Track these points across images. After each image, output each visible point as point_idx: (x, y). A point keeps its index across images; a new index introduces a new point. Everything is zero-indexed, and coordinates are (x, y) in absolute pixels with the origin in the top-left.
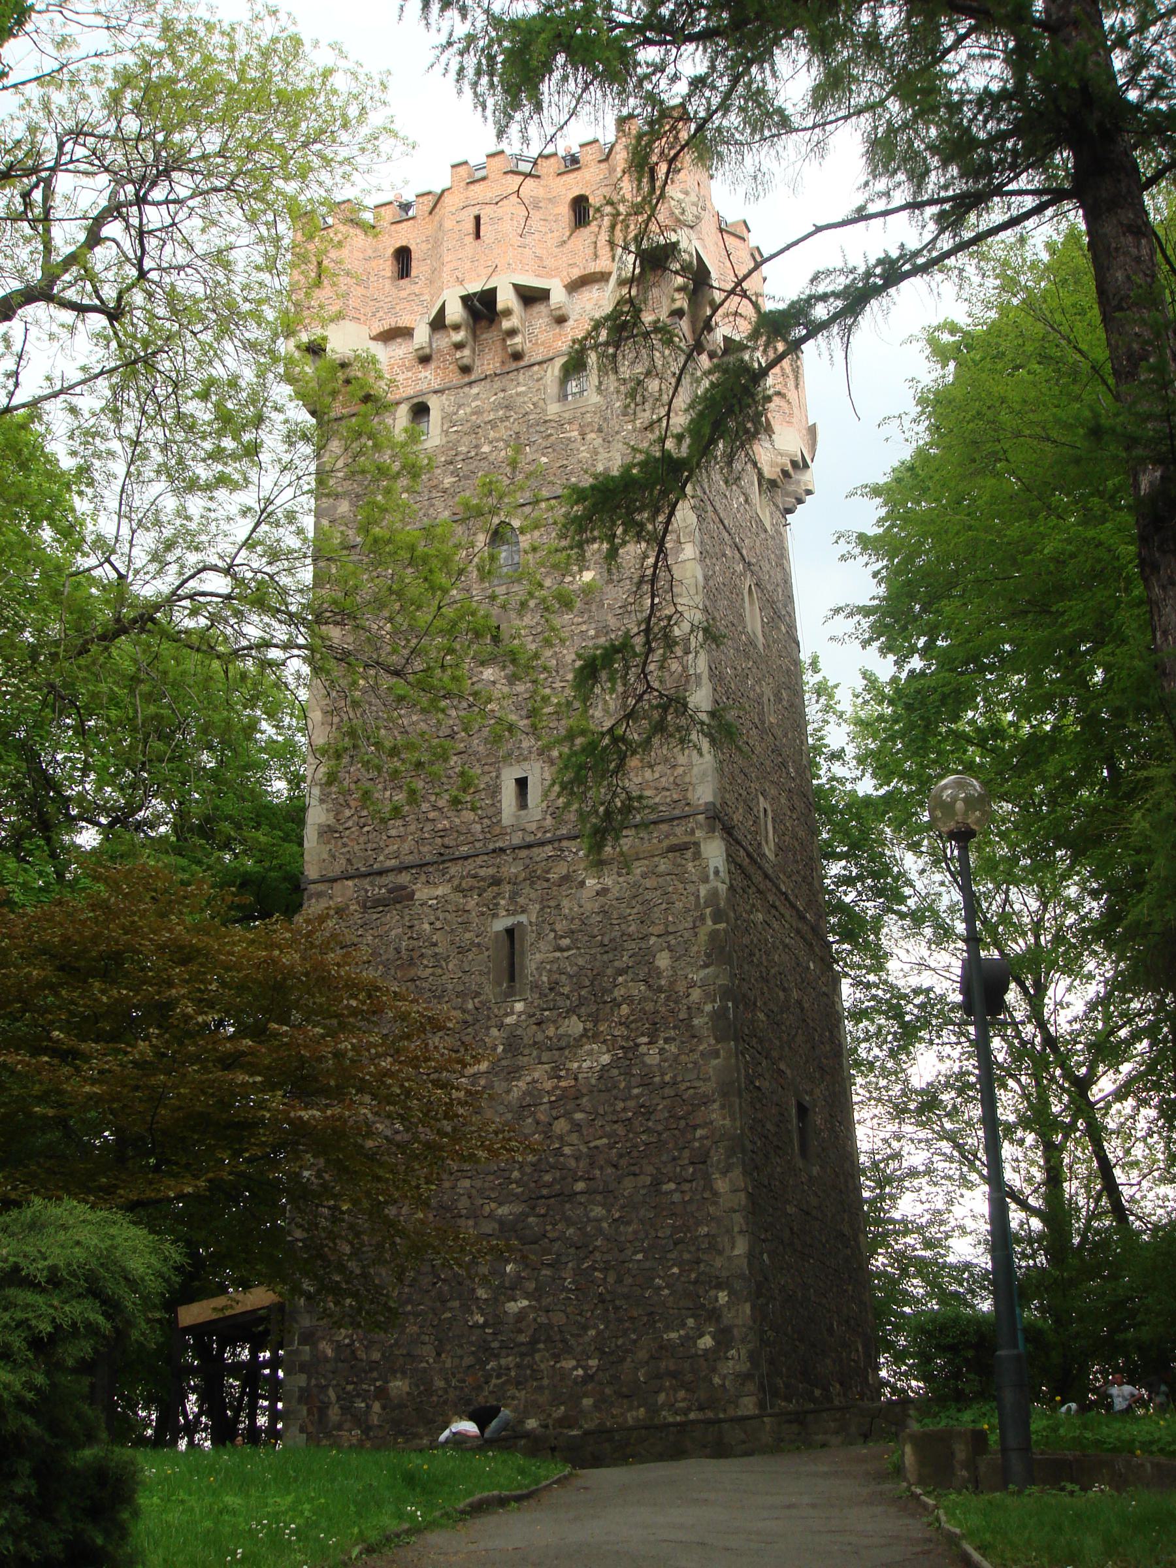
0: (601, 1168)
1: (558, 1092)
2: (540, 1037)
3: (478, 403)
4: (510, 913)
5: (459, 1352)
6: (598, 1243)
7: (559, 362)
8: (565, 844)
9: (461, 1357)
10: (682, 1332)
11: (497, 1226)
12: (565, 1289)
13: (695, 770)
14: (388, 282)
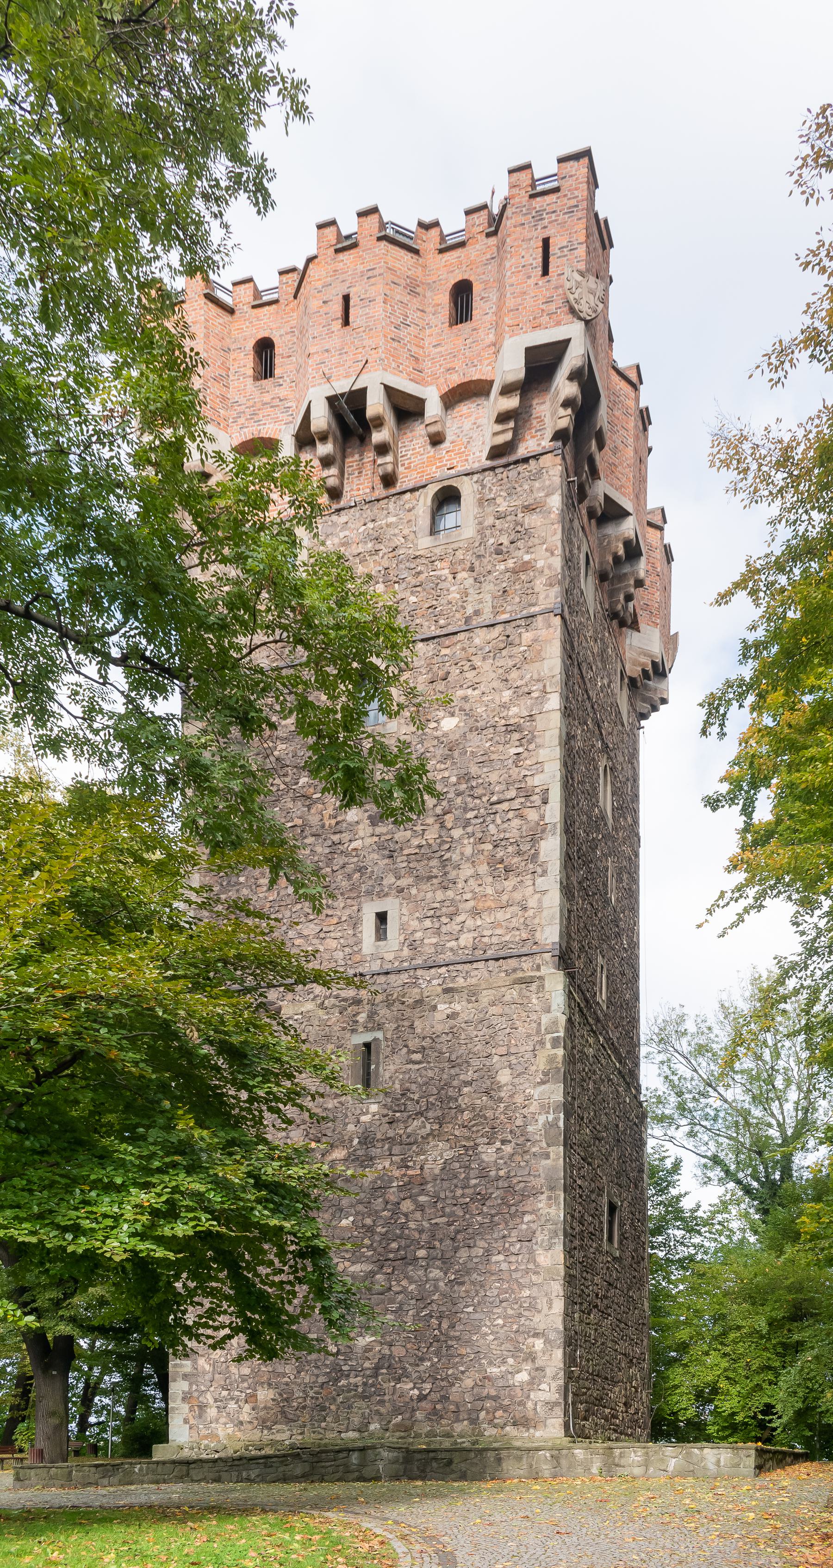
0: (441, 1241)
1: (406, 1179)
2: (391, 1133)
3: (347, 533)
4: (367, 1029)
5: (316, 1371)
6: (435, 1297)
7: (433, 489)
8: (419, 972)
9: (317, 1376)
10: (503, 1369)
13: (545, 913)
14: (250, 381)
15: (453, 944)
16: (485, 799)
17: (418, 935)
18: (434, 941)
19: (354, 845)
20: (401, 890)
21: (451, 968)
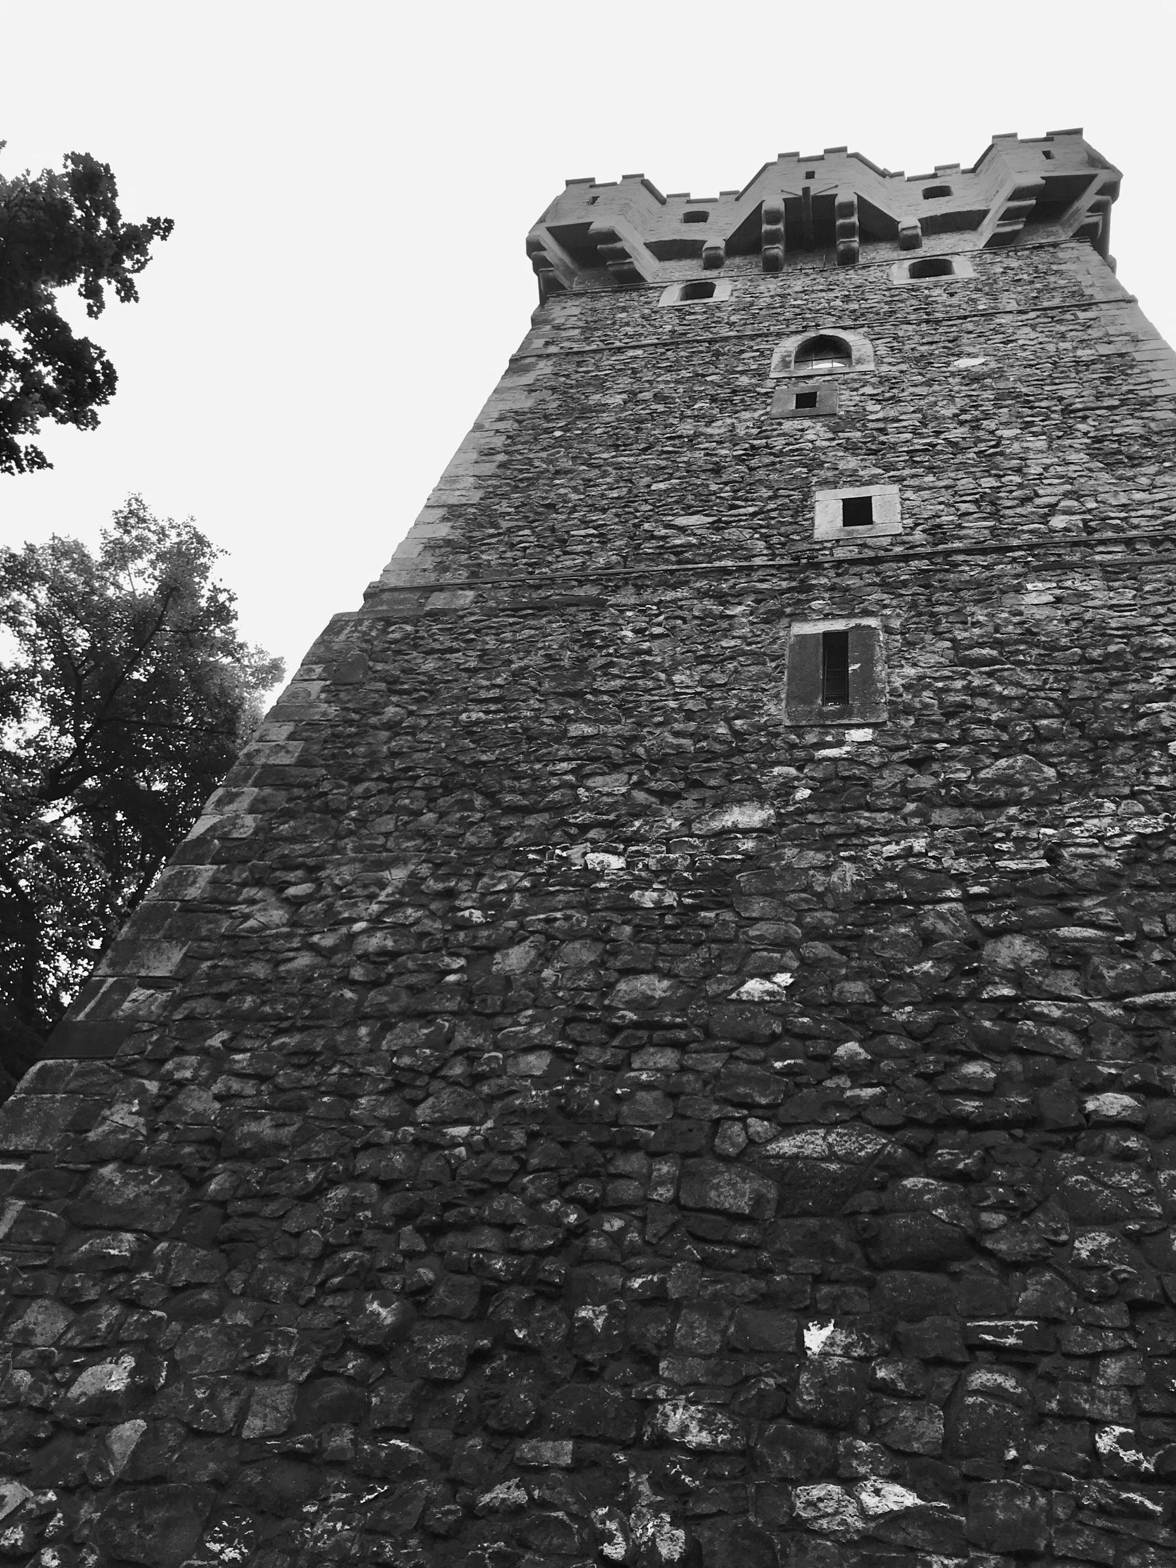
11: (772, 1194)
12: (1097, 1463)
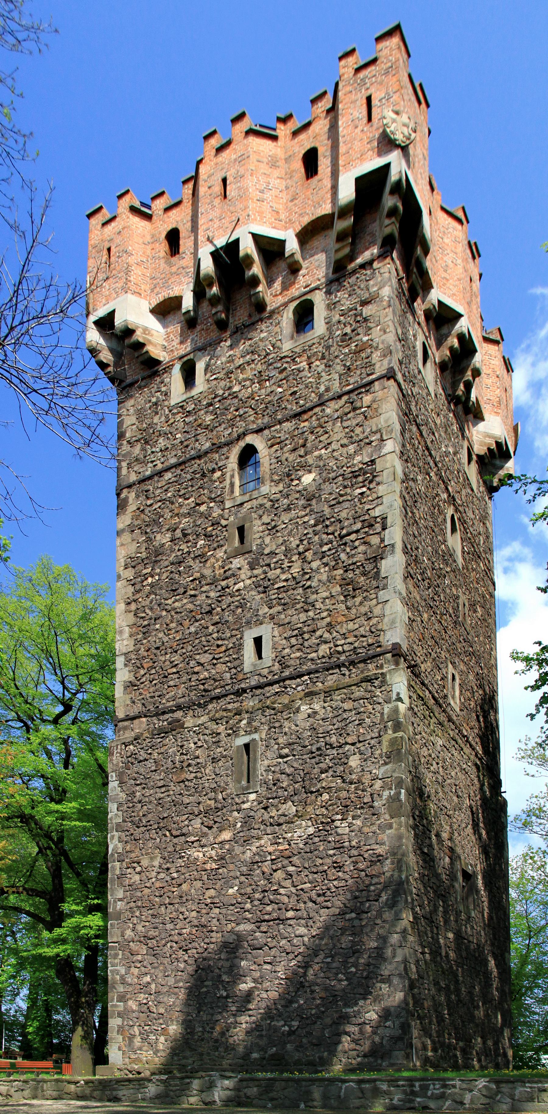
15: (314, 655)
16: (336, 534)
17: (287, 651)
18: (298, 654)
19: (237, 587)
20: (272, 617)
21: (312, 676)
